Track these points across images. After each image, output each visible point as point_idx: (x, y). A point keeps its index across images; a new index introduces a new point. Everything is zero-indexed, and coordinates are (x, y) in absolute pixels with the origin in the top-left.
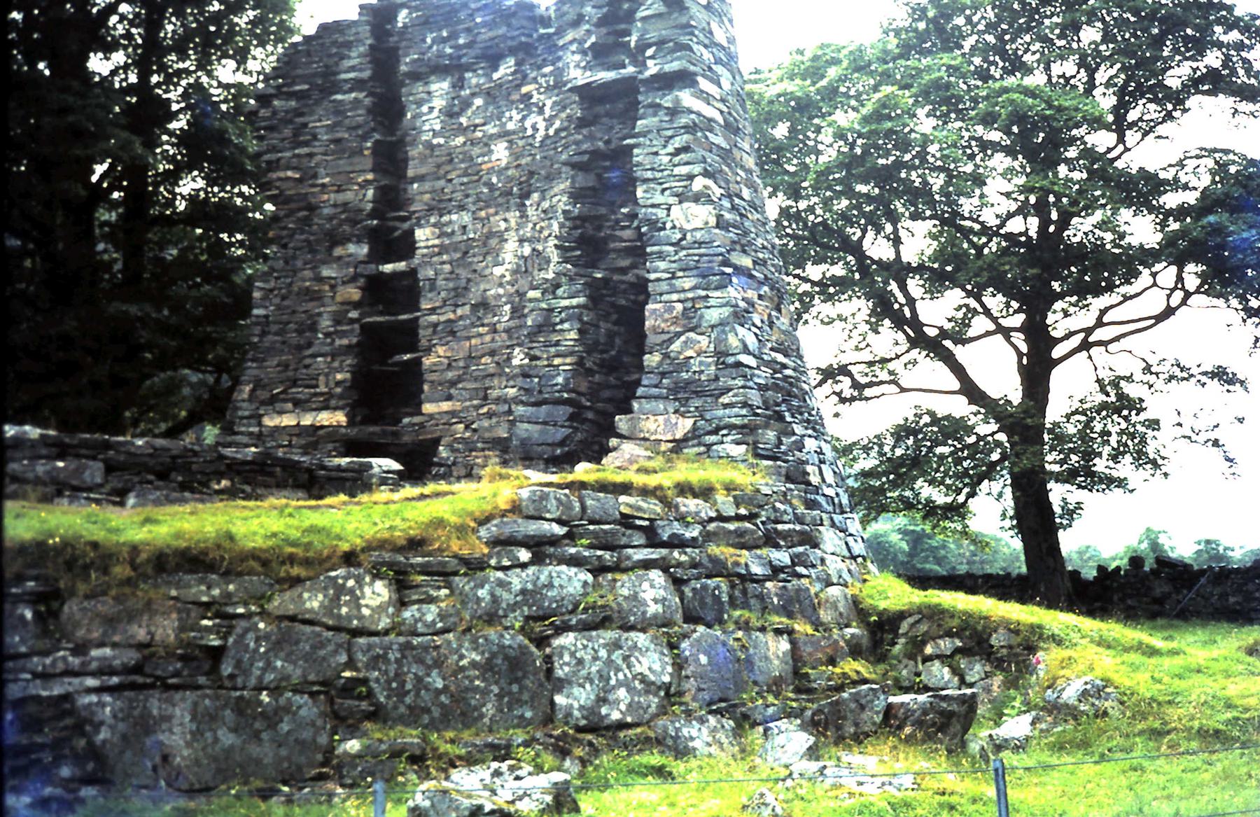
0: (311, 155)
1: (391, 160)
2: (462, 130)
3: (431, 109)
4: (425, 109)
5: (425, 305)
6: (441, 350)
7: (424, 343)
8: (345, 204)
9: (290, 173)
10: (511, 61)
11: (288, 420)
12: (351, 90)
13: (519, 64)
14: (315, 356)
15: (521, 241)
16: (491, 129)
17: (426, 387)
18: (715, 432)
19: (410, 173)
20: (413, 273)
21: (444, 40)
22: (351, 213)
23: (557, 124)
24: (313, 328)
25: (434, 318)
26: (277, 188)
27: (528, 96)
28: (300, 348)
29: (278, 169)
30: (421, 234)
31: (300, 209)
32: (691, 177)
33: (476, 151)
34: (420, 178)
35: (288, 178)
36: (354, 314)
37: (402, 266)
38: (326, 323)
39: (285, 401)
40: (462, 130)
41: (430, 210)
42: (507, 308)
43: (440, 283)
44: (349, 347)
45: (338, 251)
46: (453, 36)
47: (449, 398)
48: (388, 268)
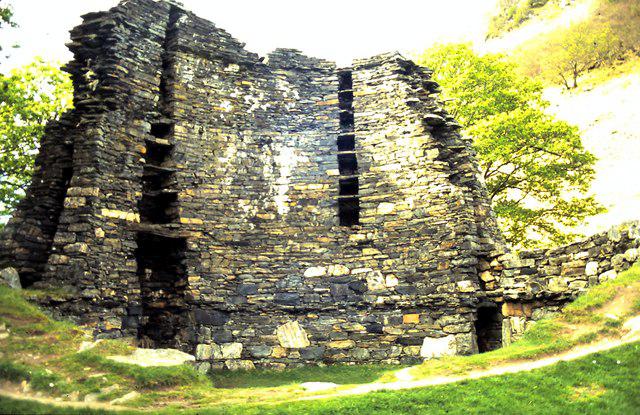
3: (189, 69)
4: (186, 67)
6: (189, 192)
9: (124, 70)
13: (240, 71)
14: (124, 178)
16: (221, 92)
22: (146, 105)
26: (116, 74)
27: (247, 87)
28: (117, 172)
29: (118, 64)
30: (179, 129)
31: (125, 92)
33: (210, 99)
34: (181, 100)
35: (122, 71)
37: (165, 142)
38: (130, 162)
39: (112, 202)
41: (184, 118)
42: (231, 179)
45: (136, 122)
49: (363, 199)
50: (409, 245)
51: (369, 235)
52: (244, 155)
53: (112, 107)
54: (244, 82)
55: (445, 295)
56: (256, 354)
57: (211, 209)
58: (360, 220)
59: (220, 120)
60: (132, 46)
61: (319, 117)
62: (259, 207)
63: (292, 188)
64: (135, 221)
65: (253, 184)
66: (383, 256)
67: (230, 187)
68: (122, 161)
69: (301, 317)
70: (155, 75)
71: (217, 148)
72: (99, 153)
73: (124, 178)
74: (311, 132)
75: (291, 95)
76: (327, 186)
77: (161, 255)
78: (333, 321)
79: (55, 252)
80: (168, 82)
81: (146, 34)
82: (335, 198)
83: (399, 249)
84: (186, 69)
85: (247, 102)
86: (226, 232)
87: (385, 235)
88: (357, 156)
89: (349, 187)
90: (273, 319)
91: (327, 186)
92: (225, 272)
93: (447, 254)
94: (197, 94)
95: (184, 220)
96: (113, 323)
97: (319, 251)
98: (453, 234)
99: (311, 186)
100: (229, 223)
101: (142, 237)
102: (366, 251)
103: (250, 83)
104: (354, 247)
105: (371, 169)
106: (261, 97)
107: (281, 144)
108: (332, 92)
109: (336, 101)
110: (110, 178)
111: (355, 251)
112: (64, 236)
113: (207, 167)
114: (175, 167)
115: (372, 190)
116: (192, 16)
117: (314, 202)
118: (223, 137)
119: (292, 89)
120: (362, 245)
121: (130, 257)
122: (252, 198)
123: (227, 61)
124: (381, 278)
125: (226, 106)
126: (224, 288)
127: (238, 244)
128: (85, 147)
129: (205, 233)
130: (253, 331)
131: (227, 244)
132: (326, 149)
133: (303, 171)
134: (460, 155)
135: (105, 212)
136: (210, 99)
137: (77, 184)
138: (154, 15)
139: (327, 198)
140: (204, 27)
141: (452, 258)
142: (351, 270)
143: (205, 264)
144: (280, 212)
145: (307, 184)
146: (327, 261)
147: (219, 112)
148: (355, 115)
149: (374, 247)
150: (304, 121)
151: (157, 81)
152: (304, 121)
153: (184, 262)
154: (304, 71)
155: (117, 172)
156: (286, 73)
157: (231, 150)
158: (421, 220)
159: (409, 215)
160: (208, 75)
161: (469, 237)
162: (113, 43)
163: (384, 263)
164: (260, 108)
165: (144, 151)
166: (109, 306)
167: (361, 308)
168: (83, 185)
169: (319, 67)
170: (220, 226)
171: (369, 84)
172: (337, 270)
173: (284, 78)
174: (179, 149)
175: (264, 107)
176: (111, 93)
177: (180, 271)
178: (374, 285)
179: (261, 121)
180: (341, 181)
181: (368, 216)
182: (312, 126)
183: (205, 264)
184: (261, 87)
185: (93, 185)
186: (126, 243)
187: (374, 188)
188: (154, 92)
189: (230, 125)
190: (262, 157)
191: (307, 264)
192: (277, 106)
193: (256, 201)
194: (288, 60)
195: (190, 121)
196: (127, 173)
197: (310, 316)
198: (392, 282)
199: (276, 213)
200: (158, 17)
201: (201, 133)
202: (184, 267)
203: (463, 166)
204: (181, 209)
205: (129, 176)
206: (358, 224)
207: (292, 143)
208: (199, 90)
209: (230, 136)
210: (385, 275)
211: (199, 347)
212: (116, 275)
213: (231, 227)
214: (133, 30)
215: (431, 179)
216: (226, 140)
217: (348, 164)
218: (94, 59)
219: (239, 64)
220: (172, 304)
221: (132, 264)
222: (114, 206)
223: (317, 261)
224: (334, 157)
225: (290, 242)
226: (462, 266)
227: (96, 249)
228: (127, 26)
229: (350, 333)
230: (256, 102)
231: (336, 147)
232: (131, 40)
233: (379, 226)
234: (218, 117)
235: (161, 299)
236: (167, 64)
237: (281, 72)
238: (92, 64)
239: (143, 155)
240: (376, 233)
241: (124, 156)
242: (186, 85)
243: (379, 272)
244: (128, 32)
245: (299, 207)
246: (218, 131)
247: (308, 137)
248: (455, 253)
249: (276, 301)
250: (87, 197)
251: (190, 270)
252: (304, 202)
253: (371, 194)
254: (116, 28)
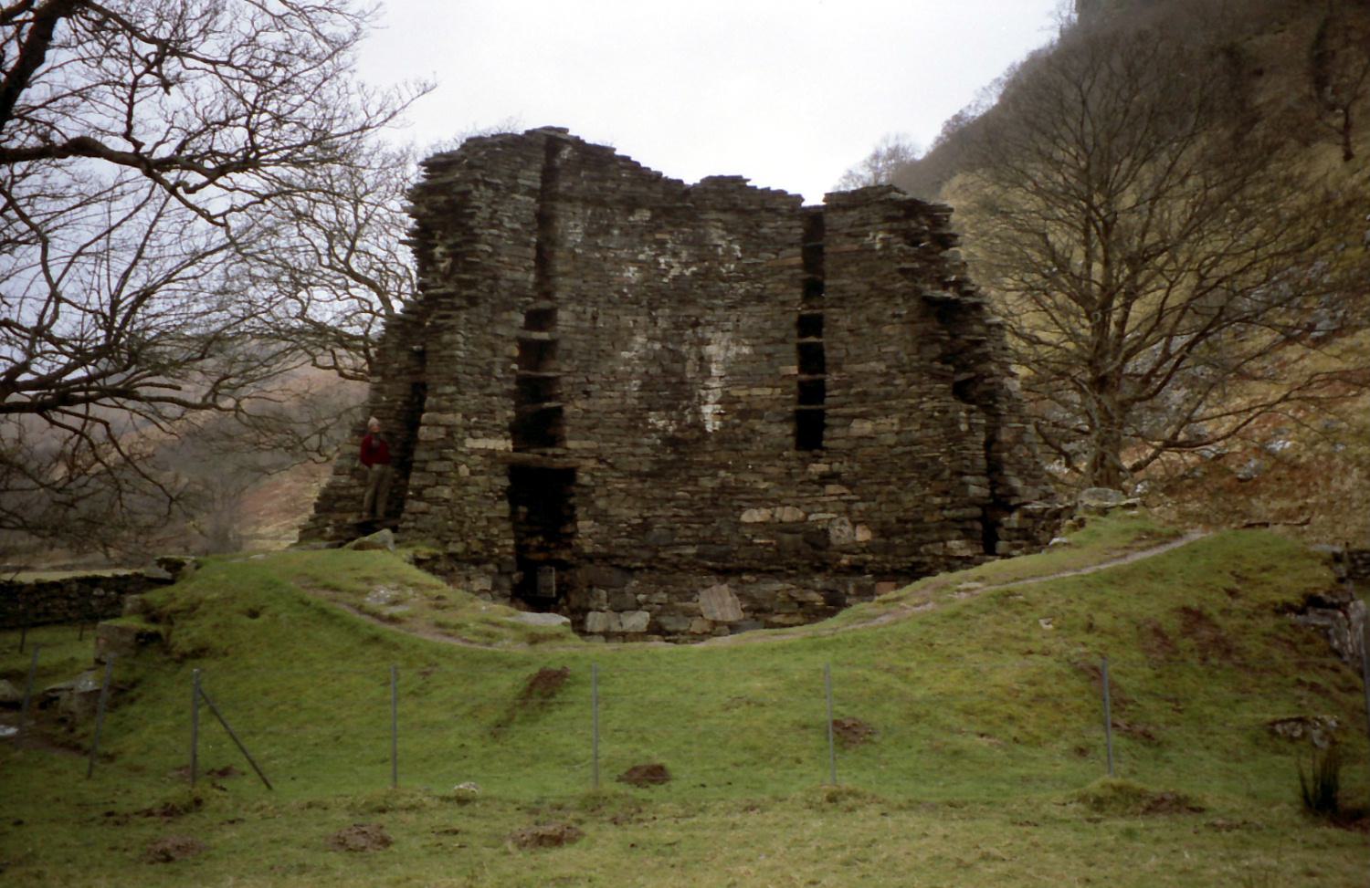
2: (599, 248)
3: (576, 226)
4: (571, 223)
6: (579, 404)
7: (565, 397)
8: (514, 281)
10: (647, 214)
11: (481, 444)
15: (652, 339)
16: (624, 254)
21: (593, 179)
23: (694, 269)
25: (571, 379)
30: (563, 315)
33: (608, 266)
34: (565, 274)
37: (544, 336)
38: (498, 372)
39: (477, 428)
41: (571, 299)
43: (575, 354)
45: (505, 316)
46: (603, 179)
47: (587, 439)
49: (830, 412)
50: (888, 483)
51: (836, 466)
52: (657, 346)
53: (473, 301)
54: (658, 236)
55: (928, 559)
56: (668, 628)
57: (610, 427)
58: (824, 443)
59: (623, 295)
60: (496, 211)
61: (771, 285)
62: (679, 423)
63: (726, 394)
64: (507, 450)
65: (672, 387)
66: (853, 497)
67: (637, 394)
68: (488, 373)
69: (733, 580)
70: (527, 245)
71: (620, 338)
72: (460, 368)
74: (758, 309)
75: (729, 252)
76: (778, 391)
77: (541, 495)
78: (778, 586)
79: (412, 497)
80: (547, 248)
81: (513, 189)
82: (790, 409)
83: (875, 488)
84: (573, 230)
85: (663, 266)
86: (631, 459)
87: (857, 467)
88: (825, 347)
89: (811, 392)
90: (694, 579)
91: (778, 391)
92: (628, 513)
93: (938, 500)
94: (588, 263)
95: (571, 444)
96: (482, 583)
97: (763, 486)
98: (947, 473)
99: (756, 391)
100: (635, 445)
101: (517, 472)
102: (831, 489)
103: (667, 237)
104: (814, 482)
105: (844, 367)
106: (684, 255)
107: (712, 328)
108: (791, 245)
109: (798, 260)
110: (475, 397)
111: (815, 487)
112: (421, 478)
113: (605, 366)
114: (559, 370)
115: (843, 399)
116: (578, 143)
117: (759, 414)
118: (628, 321)
119: (731, 242)
120: (825, 479)
121: (500, 498)
122: (669, 408)
123: (632, 205)
124: (847, 529)
125: (631, 273)
126: (627, 537)
127: (649, 475)
128: (441, 359)
129: (601, 461)
130: (665, 596)
131: (633, 474)
132: (778, 335)
133: (745, 368)
134: (978, 351)
135: (470, 443)
136: (608, 266)
137: (432, 409)
138: (523, 157)
139: (779, 408)
140: (600, 159)
141: (942, 507)
142: (807, 514)
143: (601, 503)
144: (709, 428)
145: (750, 387)
146: (773, 500)
147: (621, 284)
148: (827, 283)
149: (842, 483)
150: (747, 291)
151: (531, 252)
152: (747, 291)
153: (572, 501)
154: (750, 213)
155: (481, 387)
156: (722, 216)
157: (640, 339)
158: (908, 449)
159: (891, 440)
161: (967, 478)
162: (472, 216)
163: (854, 507)
164: (682, 275)
165: (516, 353)
166: (477, 563)
167: (818, 570)
168: (441, 410)
169: (773, 206)
170: (623, 450)
171: (849, 235)
172: (787, 514)
173: (719, 224)
174: (565, 345)
175: (688, 273)
176: (471, 284)
177: (566, 512)
178: (838, 537)
179: (681, 294)
180: (801, 384)
181: (835, 437)
182: (761, 299)
183: (601, 503)
184: (685, 242)
185: (455, 411)
186: (496, 481)
187: (847, 395)
189: (637, 302)
190: (684, 348)
191: (744, 504)
192: (708, 270)
193: (674, 413)
194: (728, 196)
195: (580, 302)
196: (495, 387)
197: (745, 577)
198: (863, 535)
199: (703, 429)
201: (594, 318)
202: (573, 508)
203: (981, 367)
204: (568, 429)
205: (497, 390)
206: (823, 449)
207: (729, 325)
208: (591, 255)
209: (639, 319)
210: (855, 524)
211: (591, 615)
212: (484, 523)
213: (638, 451)
215: (925, 388)
216: (631, 324)
217: (812, 359)
218: (445, 230)
219: (651, 209)
220: (556, 557)
221: (503, 507)
222: (480, 433)
223: (759, 501)
224: (791, 349)
225: (722, 473)
226: (955, 520)
227: (460, 492)
228: (487, 184)
229: (801, 604)
230: (675, 266)
231: (795, 332)
232: (494, 202)
233: (850, 454)
234: (618, 292)
235: (540, 549)
236: (544, 220)
237: (713, 215)
238: (442, 238)
240: (845, 464)
241: (490, 364)
242: (572, 251)
243: (846, 519)
244: (490, 193)
245: (737, 421)
246: (619, 312)
247: (751, 317)
248: (948, 500)
249: (698, 555)
250: (447, 426)
251: (580, 512)
252: (744, 415)
253: (842, 405)
254: (475, 193)
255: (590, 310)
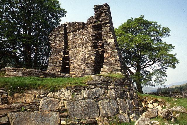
0: (56, 42)
1: (66, 43)
2: (75, 38)
4: (70, 36)
5: (70, 60)
6: (72, 65)
10: (81, 30)
12: (61, 34)
13: (82, 30)
15: (82, 51)
16: (79, 38)
17: (70, 70)
18: (116, 70)
19: (68, 44)
20: (69, 56)
21: (73, 28)
22: (61, 49)
23: (87, 37)
24: (56, 63)
27: (84, 34)
28: (55, 66)
32: (110, 35)
36: (61, 61)
37: (67, 55)
38: (58, 63)
40: (75, 38)
42: (81, 60)
44: (61, 65)
45: (59, 54)
46: (74, 27)
47: (73, 71)
48: (66, 56)
52: (83, 52)
60: (56, 39)
73: (56, 67)
81: (59, 35)
84: (70, 37)
118: (79, 49)
151: (63, 43)
157: (81, 52)
160: (76, 35)
174: (70, 56)
188: (63, 45)
200: (61, 29)
201: (75, 50)
214: (55, 35)
228: (54, 35)
234: (78, 45)
239: (62, 60)
244: (54, 36)
255: (74, 49)
